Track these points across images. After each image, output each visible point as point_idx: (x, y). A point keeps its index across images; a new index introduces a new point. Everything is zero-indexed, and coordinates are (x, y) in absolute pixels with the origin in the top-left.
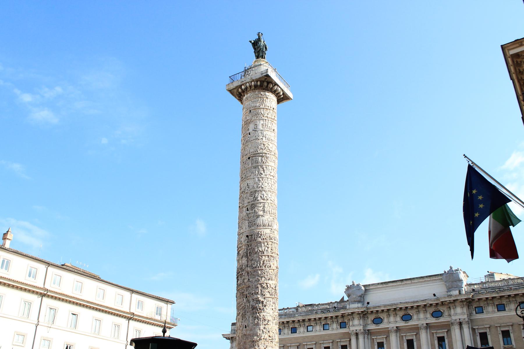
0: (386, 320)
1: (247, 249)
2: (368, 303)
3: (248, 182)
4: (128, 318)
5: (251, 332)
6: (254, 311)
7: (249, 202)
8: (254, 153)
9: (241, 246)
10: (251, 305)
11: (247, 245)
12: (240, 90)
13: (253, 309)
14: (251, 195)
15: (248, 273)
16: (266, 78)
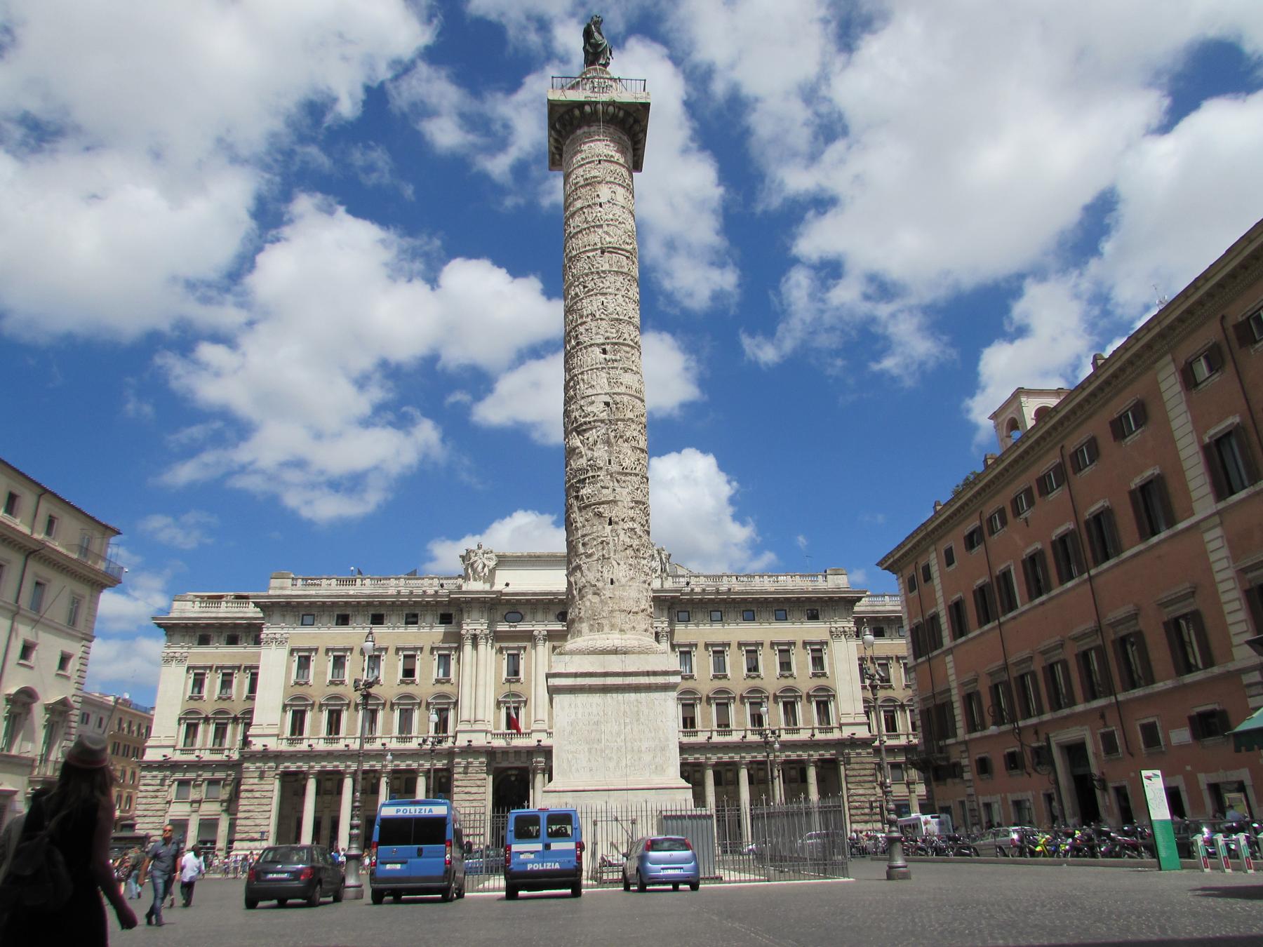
0: (528, 617)
1: (607, 429)
2: (507, 585)
3: (602, 298)
4: (25, 550)
5: (625, 594)
6: (628, 552)
7: (608, 338)
8: (614, 245)
9: (592, 419)
10: (621, 539)
11: (607, 422)
12: (577, 112)
13: (626, 549)
14: (613, 326)
15: (611, 476)
16: (638, 109)
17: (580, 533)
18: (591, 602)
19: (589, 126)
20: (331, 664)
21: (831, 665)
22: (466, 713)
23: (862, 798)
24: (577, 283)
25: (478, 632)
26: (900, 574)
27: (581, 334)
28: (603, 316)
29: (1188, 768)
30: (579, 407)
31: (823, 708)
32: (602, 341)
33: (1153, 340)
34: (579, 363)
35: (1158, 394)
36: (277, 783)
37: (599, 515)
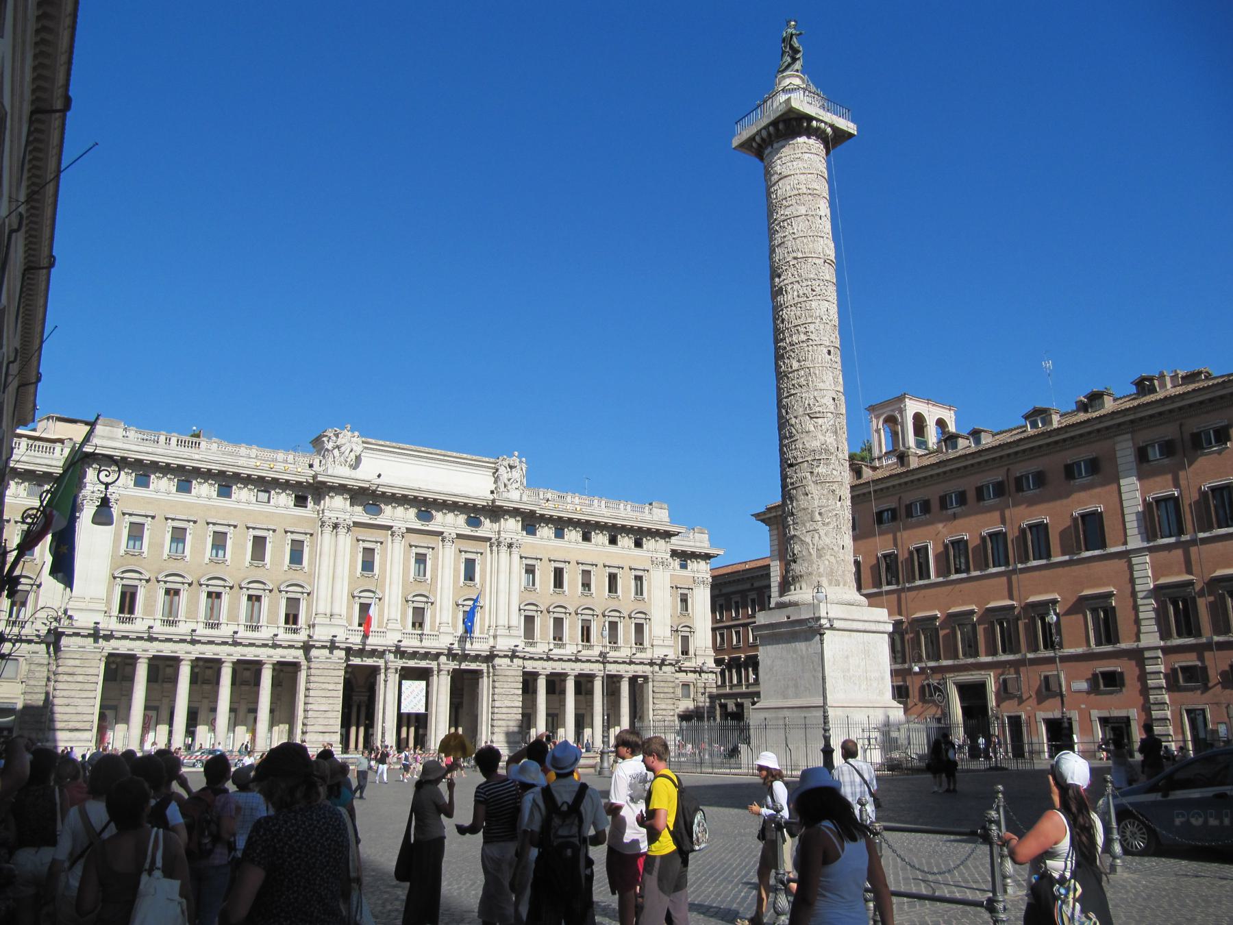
2: (379, 476)
16: (844, 136)
17: (816, 503)
18: (829, 562)
19: (809, 138)
20: (168, 537)
21: (649, 591)
22: (323, 606)
23: (664, 713)
24: (804, 284)
25: (340, 521)
26: (775, 526)
27: (812, 332)
28: (828, 321)
29: (1083, 706)
30: (812, 397)
31: (639, 628)
32: (828, 344)
33: (1124, 423)
34: (810, 358)
35: (1113, 458)
36: (103, 666)
37: (833, 491)
